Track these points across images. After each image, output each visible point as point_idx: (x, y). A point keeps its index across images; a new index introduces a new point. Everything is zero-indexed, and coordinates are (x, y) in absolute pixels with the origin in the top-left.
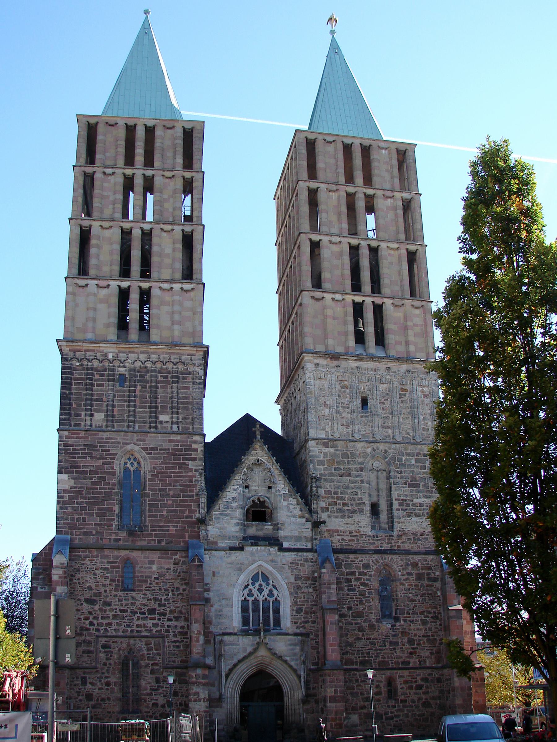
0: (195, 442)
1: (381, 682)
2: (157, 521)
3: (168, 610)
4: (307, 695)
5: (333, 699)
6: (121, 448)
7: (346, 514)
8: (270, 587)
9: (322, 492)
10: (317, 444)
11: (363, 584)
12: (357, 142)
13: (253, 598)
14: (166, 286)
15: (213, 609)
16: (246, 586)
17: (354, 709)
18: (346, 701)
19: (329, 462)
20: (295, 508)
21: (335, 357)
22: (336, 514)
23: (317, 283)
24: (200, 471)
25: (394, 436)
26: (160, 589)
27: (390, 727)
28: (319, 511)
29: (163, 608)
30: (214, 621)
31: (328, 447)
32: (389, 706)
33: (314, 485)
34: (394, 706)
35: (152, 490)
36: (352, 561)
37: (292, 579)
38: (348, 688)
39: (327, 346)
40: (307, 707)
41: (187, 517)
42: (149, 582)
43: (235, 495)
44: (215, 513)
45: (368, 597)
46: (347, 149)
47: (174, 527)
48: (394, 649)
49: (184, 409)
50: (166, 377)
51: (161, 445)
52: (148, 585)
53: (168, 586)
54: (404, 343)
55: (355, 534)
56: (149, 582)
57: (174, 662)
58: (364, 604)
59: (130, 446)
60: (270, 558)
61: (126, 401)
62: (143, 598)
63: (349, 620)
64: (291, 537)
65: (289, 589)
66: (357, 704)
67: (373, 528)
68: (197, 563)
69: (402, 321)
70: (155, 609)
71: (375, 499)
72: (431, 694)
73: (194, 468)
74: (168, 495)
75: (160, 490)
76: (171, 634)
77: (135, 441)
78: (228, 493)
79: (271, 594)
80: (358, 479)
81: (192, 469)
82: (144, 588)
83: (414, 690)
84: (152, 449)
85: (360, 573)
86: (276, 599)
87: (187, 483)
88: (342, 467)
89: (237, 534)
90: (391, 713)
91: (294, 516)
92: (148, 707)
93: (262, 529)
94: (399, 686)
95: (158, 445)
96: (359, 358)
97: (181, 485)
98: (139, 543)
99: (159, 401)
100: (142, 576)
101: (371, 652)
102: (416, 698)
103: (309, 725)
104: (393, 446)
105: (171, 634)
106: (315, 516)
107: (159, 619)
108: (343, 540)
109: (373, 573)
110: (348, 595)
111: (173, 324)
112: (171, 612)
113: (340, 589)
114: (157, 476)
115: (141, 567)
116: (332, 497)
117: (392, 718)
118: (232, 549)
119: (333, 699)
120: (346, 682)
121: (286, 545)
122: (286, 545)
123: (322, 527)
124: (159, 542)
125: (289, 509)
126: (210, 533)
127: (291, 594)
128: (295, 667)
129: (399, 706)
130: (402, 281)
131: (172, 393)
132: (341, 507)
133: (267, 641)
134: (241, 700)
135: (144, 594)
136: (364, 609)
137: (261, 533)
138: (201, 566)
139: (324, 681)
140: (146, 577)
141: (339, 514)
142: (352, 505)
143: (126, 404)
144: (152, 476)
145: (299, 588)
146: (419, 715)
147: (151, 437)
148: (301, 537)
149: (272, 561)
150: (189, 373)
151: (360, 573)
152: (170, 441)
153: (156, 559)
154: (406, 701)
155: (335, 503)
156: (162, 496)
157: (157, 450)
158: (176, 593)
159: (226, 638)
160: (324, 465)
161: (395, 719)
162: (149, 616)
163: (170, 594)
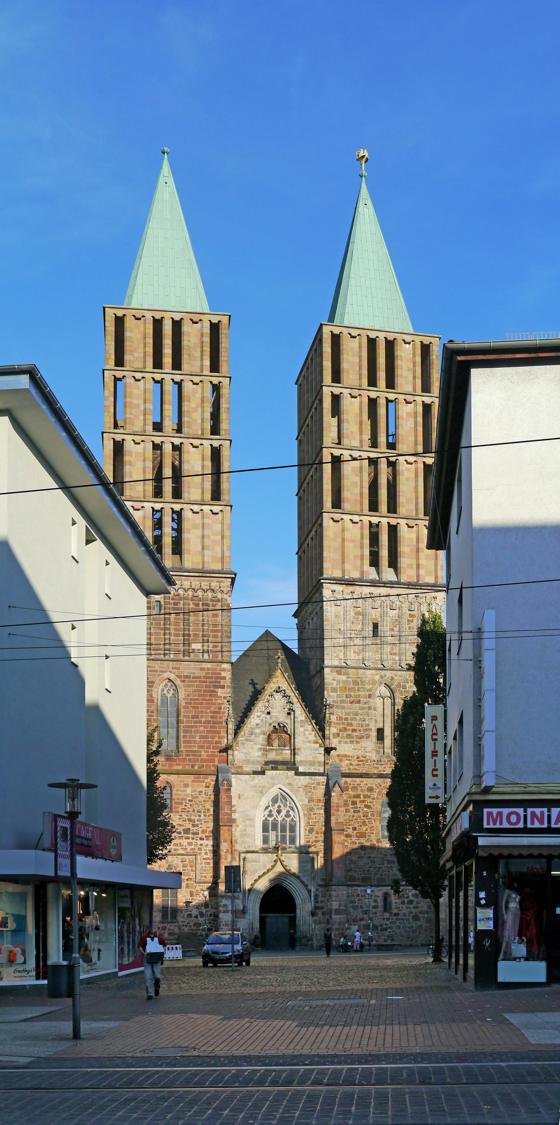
0: (224, 670)
1: (378, 897)
2: (191, 747)
3: (200, 830)
4: (316, 908)
5: (338, 912)
6: (159, 675)
7: (355, 739)
8: (288, 808)
9: (334, 718)
10: (331, 671)
11: (367, 806)
12: (382, 336)
13: (272, 819)
14: (196, 508)
15: (238, 829)
16: (267, 808)
17: (355, 920)
18: (348, 914)
19: (341, 690)
20: (310, 734)
21: (350, 583)
22: (346, 740)
23: (337, 503)
24: (229, 698)
25: (400, 663)
26: (194, 811)
27: (384, 937)
28: (331, 737)
29: (196, 828)
30: (239, 840)
31: (341, 674)
32: (384, 919)
33: (327, 712)
34: (388, 919)
35: (187, 717)
36: (358, 785)
37: (306, 802)
38: (351, 902)
39: (343, 571)
40: (316, 918)
41: (216, 743)
42: (184, 804)
43: (258, 721)
44: (240, 738)
45: (371, 819)
46: (372, 343)
47: (205, 752)
48: (391, 867)
49: (215, 636)
50: (198, 605)
51: (194, 673)
52: (183, 807)
53: (200, 807)
54: (415, 567)
55: (361, 759)
56: (184, 804)
57: (205, 877)
58: (366, 825)
59: (165, 674)
60: (287, 781)
61: (161, 629)
62: (179, 819)
63: (354, 839)
64: (306, 762)
65: (303, 810)
66: (357, 916)
67: (378, 752)
68: (226, 787)
69: (415, 543)
70: (189, 829)
71: (380, 726)
72: (420, 909)
73: (223, 695)
74: (200, 722)
75: (193, 717)
76: (203, 852)
77: (171, 669)
78: (252, 720)
79: (288, 815)
80: (367, 706)
81: (221, 697)
82: (180, 810)
83: (406, 905)
84: (186, 677)
85: (365, 796)
86: (292, 819)
87: (217, 710)
88: (353, 694)
89: (260, 759)
90: (386, 924)
91: (309, 742)
92: (183, 917)
93: (281, 753)
94: (394, 901)
95: (192, 673)
96: (373, 584)
97: (212, 712)
98: (176, 768)
99: (191, 628)
100: (178, 799)
101: (371, 869)
102: (407, 912)
103: (316, 934)
104: (399, 673)
105: (203, 852)
106: (327, 741)
107: (193, 839)
108: (351, 764)
109: (375, 796)
110: (353, 816)
111: (203, 548)
112: (203, 832)
113: (347, 811)
114: (191, 703)
115: (178, 790)
116: (343, 724)
117: (386, 929)
118: (255, 773)
119: (338, 912)
120: (349, 896)
121: (301, 769)
122: (301, 769)
123: (333, 753)
124: (193, 766)
125: (305, 735)
126: (236, 758)
127: (305, 815)
128: (306, 882)
129: (392, 919)
130: (417, 498)
131: (203, 620)
132: (350, 733)
133: (283, 858)
134: (260, 913)
135: (180, 816)
136: (367, 830)
137: (280, 758)
138: (230, 790)
139: (330, 895)
140: (182, 799)
141: (349, 740)
142: (360, 731)
143: (162, 632)
144: (186, 703)
145: (311, 809)
146: (409, 927)
147: (184, 665)
148: (314, 762)
149: (289, 784)
150: (218, 601)
151: (365, 796)
152: (202, 669)
153: (190, 783)
154: (398, 914)
155: (345, 729)
156: (195, 722)
157: (190, 678)
158: (207, 814)
159: (249, 855)
160: (337, 692)
161: (389, 930)
162: (185, 835)
163: (202, 815)
